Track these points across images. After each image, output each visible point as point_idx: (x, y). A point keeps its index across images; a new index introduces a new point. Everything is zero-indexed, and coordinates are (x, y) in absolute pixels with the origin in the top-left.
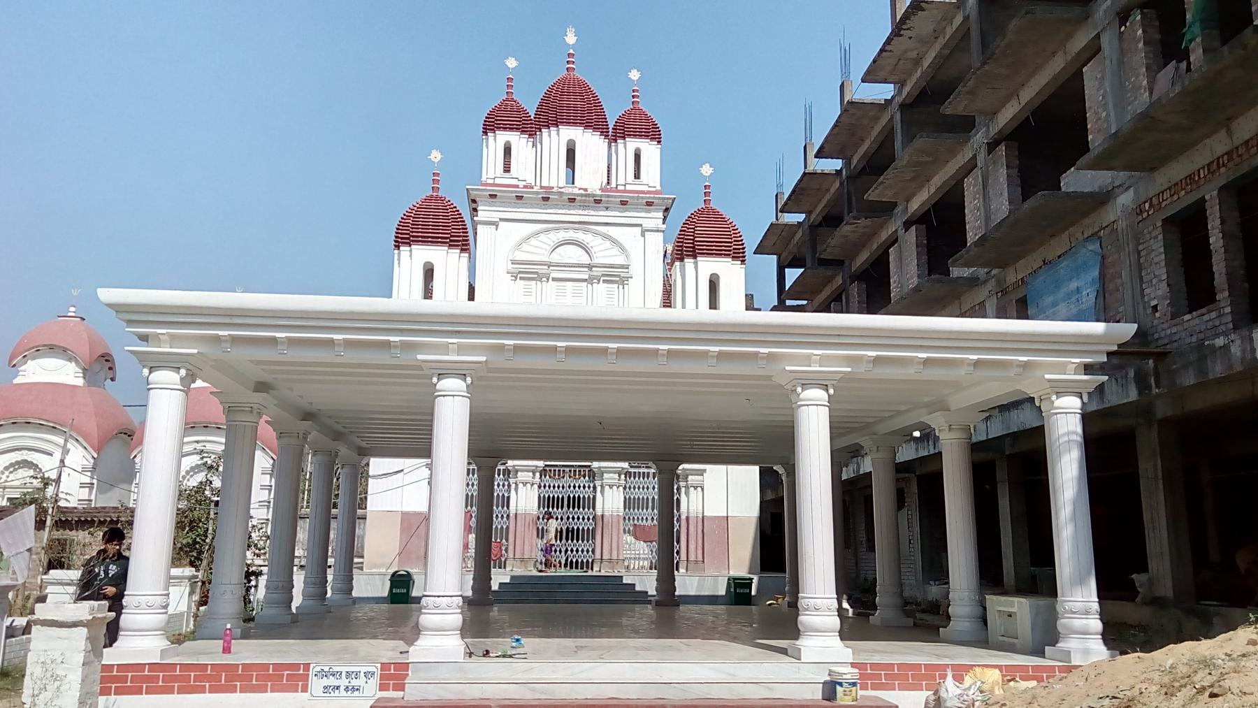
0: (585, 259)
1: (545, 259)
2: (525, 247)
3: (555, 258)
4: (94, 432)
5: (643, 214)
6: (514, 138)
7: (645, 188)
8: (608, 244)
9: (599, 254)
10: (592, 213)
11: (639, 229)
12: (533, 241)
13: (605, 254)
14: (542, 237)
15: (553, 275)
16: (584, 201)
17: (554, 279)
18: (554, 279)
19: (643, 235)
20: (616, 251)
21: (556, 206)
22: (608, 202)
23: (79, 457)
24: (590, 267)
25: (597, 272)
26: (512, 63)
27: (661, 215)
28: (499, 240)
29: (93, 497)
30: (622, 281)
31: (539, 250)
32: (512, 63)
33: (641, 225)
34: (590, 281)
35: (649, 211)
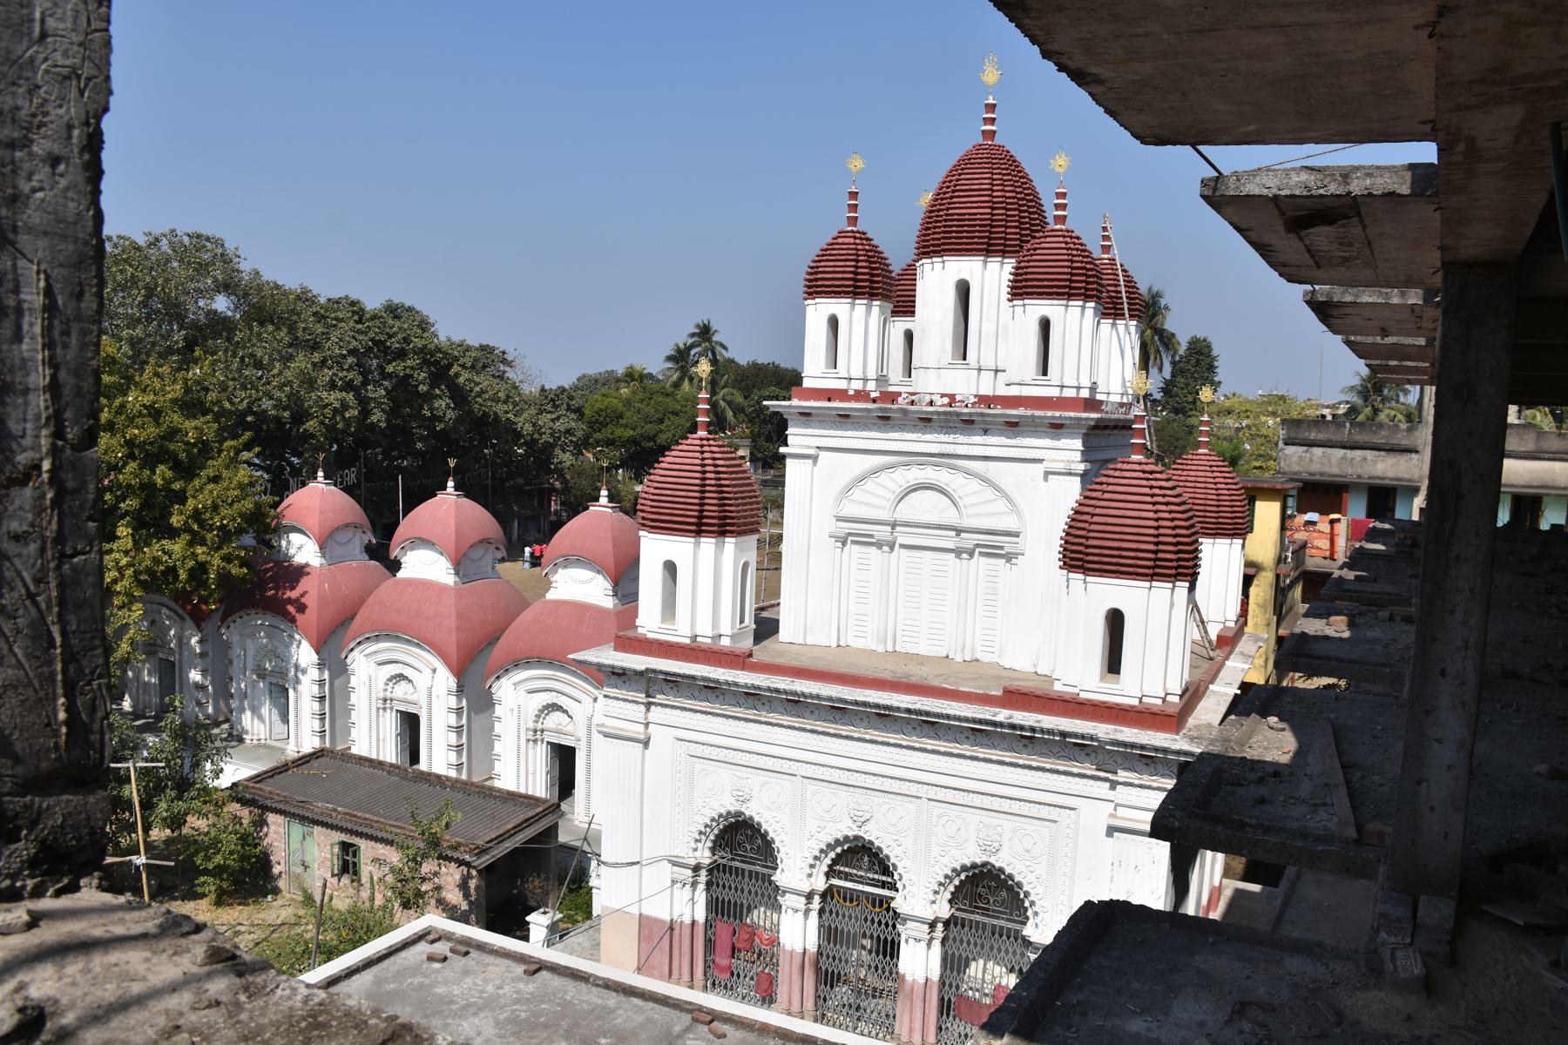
0: (950, 516)
1: (884, 515)
2: (857, 494)
3: (906, 512)
4: (453, 650)
5: (1047, 442)
6: (839, 307)
7: (1054, 392)
8: (990, 493)
9: (971, 511)
10: (961, 438)
11: (1039, 469)
12: (869, 485)
13: (980, 509)
14: (883, 478)
15: (901, 540)
16: (947, 421)
17: (902, 546)
18: (902, 546)
19: (1046, 479)
20: (1002, 505)
21: (902, 427)
22: (985, 422)
23: (445, 680)
24: (959, 531)
25: (969, 540)
26: (857, 164)
27: (1077, 444)
28: (821, 478)
29: (464, 721)
30: (1009, 557)
31: (875, 500)
32: (857, 164)
33: (1040, 461)
34: (958, 552)
35: (1057, 437)
